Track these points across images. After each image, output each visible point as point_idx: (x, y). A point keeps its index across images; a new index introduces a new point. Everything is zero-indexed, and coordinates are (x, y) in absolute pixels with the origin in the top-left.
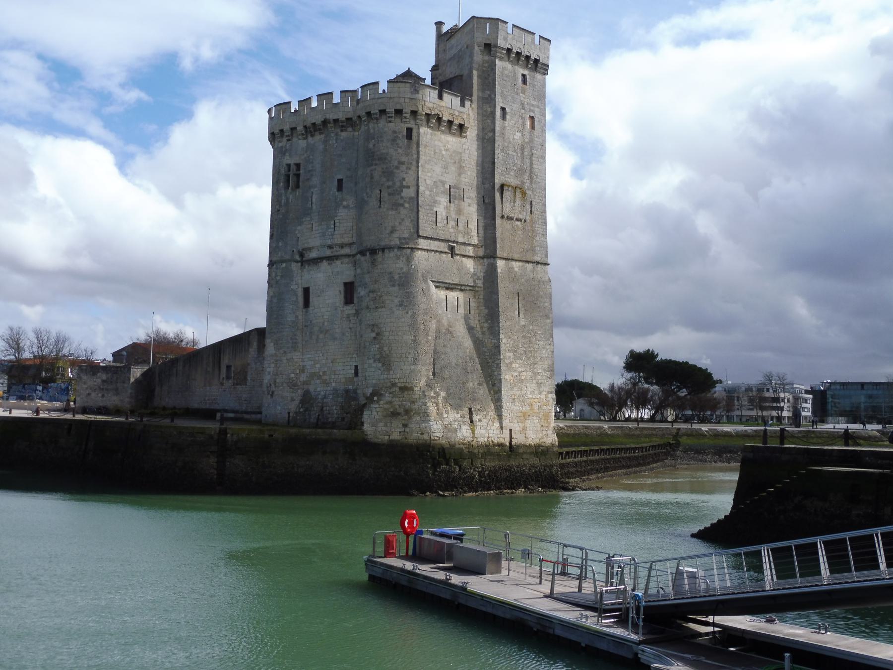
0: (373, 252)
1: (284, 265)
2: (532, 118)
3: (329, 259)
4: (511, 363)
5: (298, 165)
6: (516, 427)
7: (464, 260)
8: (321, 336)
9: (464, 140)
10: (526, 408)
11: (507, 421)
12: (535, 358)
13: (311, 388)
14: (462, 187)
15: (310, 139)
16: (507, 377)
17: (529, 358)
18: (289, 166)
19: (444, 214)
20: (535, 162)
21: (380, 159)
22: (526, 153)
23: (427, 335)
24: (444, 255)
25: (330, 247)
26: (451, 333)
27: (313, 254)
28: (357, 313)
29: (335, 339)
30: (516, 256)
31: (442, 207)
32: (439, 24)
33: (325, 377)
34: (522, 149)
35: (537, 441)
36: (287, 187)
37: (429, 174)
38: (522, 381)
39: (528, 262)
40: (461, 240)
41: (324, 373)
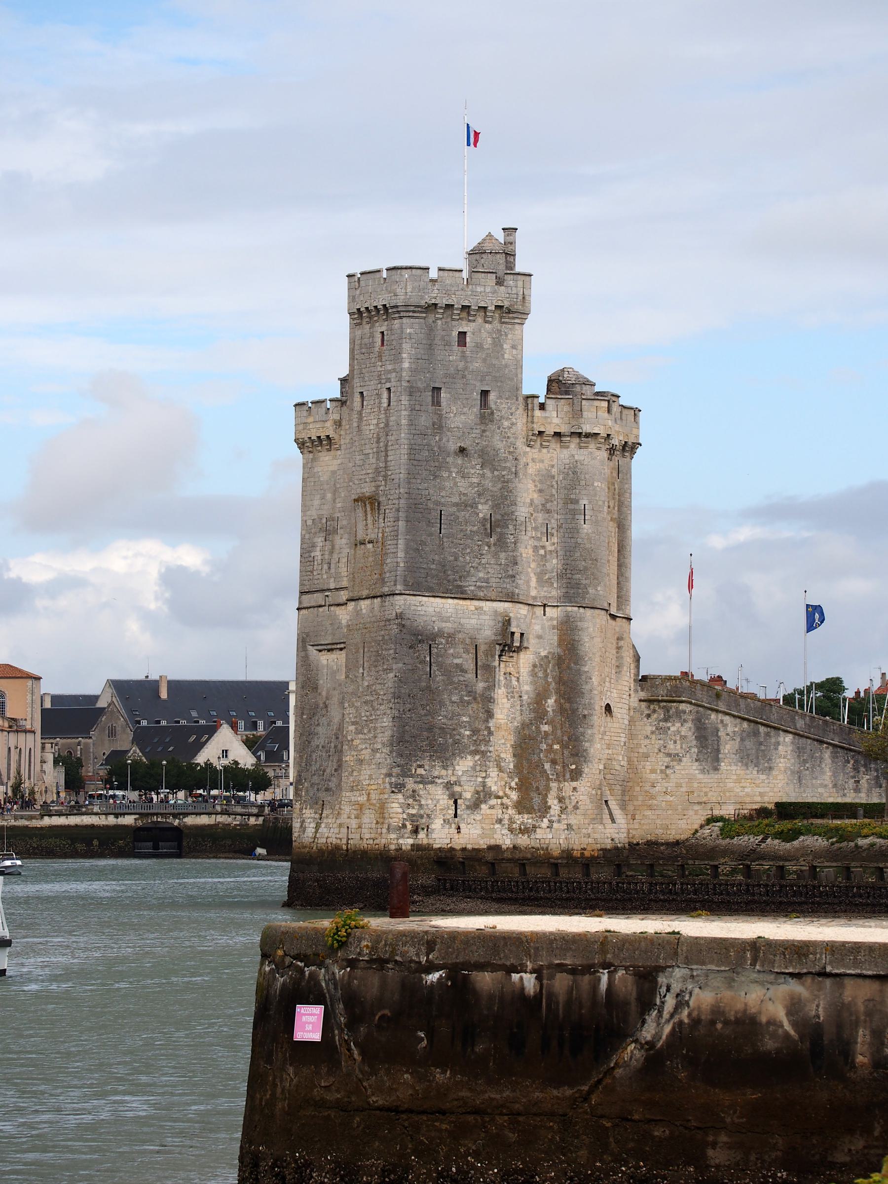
2: (389, 389)
4: (352, 740)
6: (353, 823)
7: (338, 608)
9: (339, 452)
10: (363, 799)
11: (345, 816)
12: (375, 728)
14: (336, 515)
16: (348, 758)
17: (369, 731)
19: (320, 557)
20: (390, 453)
22: (382, 444)
23: (303, 714)
24: (321, 609)
26: (326, 707)
30: (365, 593)
31: (318, 549)
34: (378, 442)
35: (371, 842)
37: (308, 513)
38: (361, 762)
39: (374, 597)
40: (332, 586)
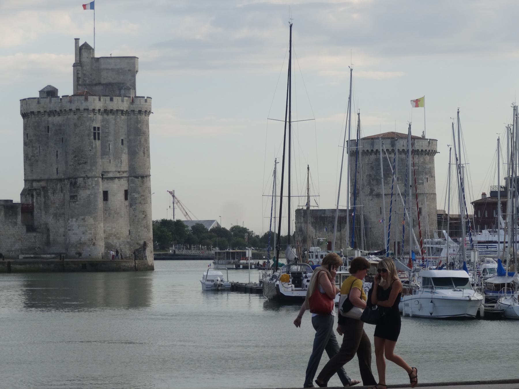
0: (143, 177)
1: (96, 179)
3: (118, 178)
5: (98, 128)
8: (115, 215)
13: (110, 241)
15: (105, 116)
18: (95, 128)
21: (143, 133)
25: (119, 172)
27: (110, 175)
28: (131, 205)
29: (122, 217)
32: (77, 40)
33: (117, 236)
36: (95, 139)
41: (117, 233)
